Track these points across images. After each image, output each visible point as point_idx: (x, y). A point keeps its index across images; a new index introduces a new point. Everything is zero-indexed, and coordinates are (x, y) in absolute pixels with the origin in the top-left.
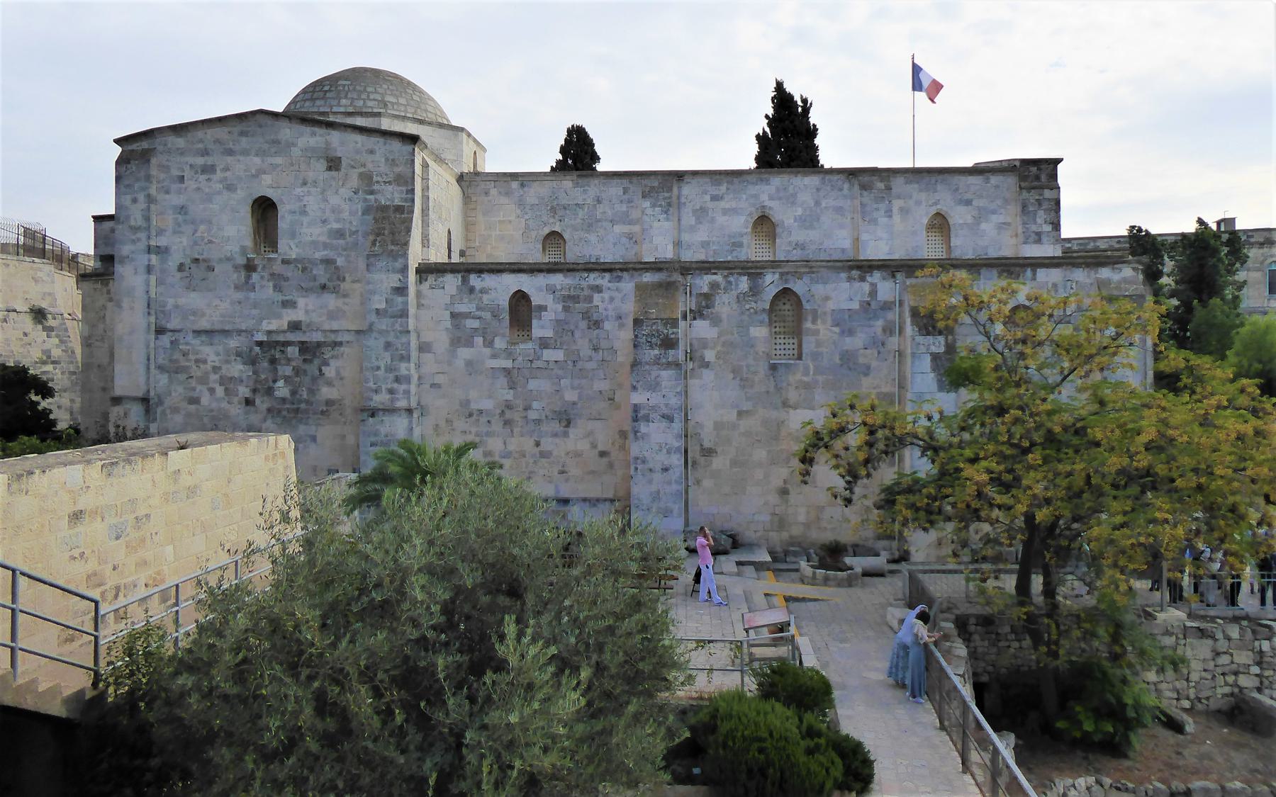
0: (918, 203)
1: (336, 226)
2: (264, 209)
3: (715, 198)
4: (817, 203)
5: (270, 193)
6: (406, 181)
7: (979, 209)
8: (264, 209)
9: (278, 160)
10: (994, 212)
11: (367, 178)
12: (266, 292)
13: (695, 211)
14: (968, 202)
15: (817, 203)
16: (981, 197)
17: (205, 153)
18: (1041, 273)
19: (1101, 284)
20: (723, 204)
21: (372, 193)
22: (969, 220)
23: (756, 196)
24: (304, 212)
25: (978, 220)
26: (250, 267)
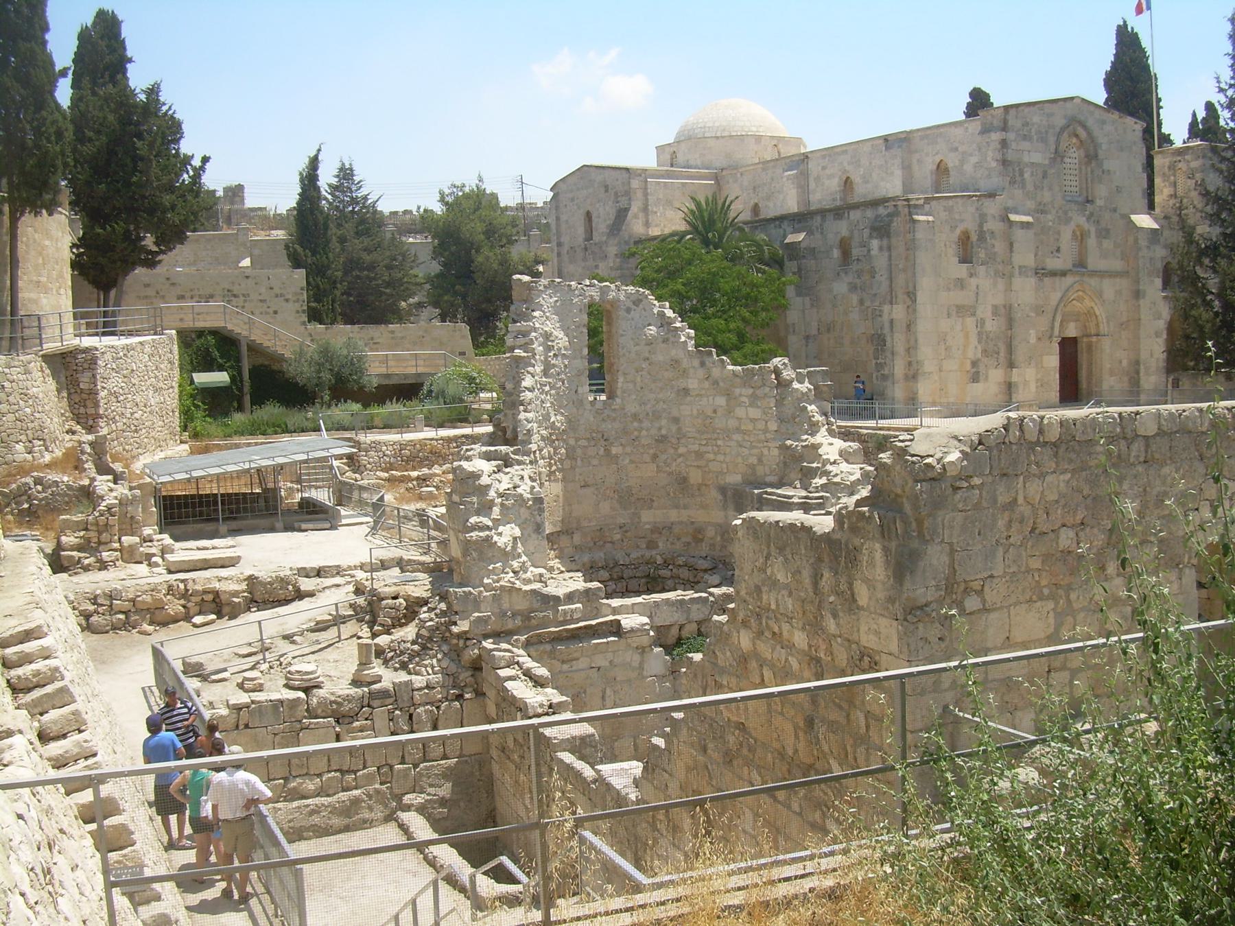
0: (927, 155)
1: (608, 222)
2: (589, 216)
3: (824, 168)
4: (870, 163)
5: (590, 208)
6: (628, 193)
7: (964, 153)
8: (589, 216)
9: (591, 190)
10: (971, 155)
11: (616, 194)
12: (590, 263)
13: (815, 179)
14: (956, 149)
15: (870, 163)
16: (963, 144)
17: (572, 191)
18: (852, 213)
19: (877, 216)
20: (828, 172)
21: (618, 202)
22: (957, 163)
23: (841, 163)
24: (599, 217)
25: (962, 162)
26: (586, 249)
